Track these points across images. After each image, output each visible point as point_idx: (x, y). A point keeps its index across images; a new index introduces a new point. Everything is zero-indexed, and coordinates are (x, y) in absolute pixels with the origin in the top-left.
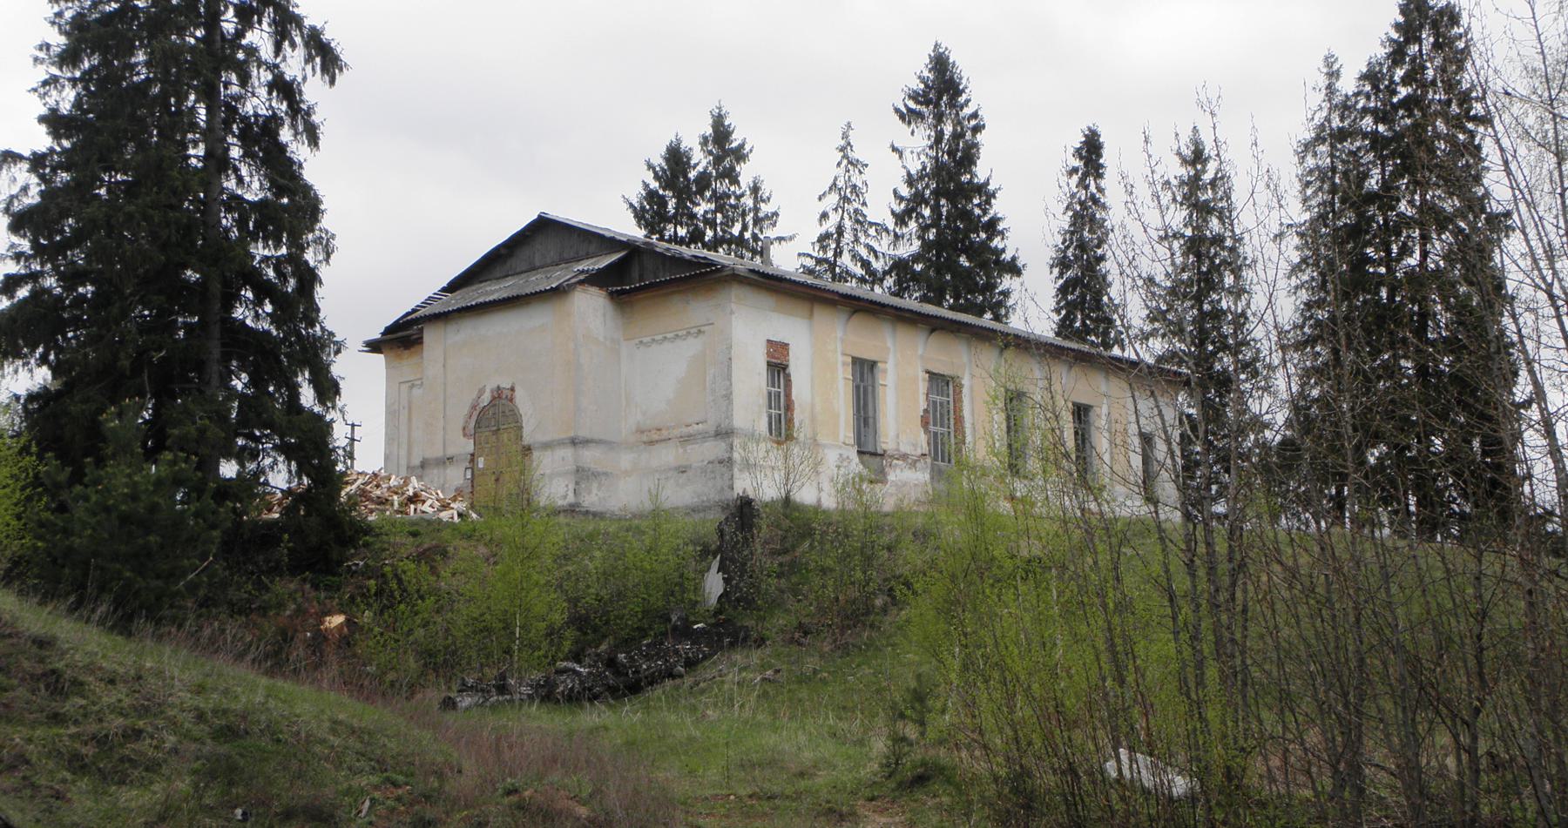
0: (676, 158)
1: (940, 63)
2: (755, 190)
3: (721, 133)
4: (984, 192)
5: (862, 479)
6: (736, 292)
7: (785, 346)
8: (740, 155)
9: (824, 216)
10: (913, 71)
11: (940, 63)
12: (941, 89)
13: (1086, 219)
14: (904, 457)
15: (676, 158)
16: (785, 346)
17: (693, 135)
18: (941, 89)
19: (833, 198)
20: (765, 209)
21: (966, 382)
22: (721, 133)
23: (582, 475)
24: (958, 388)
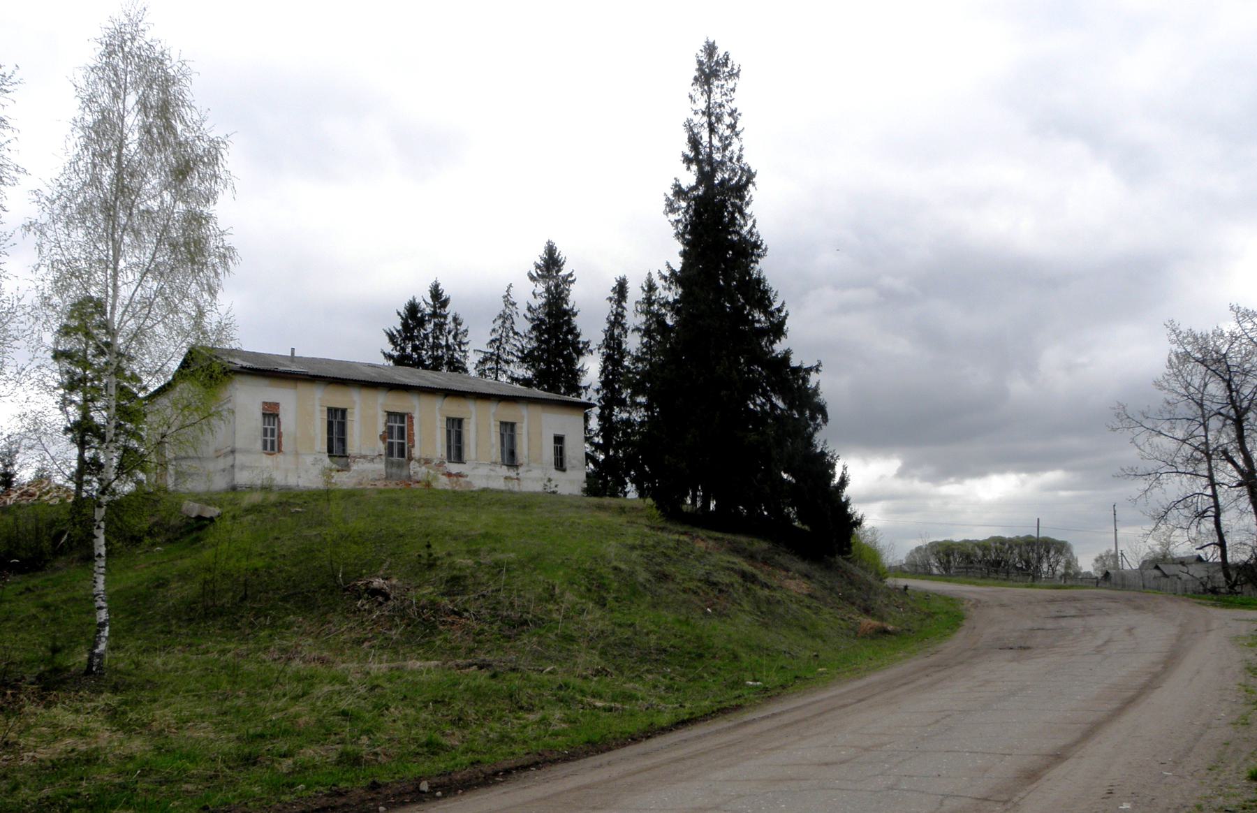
0: (413, 309)
1: (551, 250)
2: (455, 319)
3: (436, 293)
4: (571, 313)
5: (331, 470)
6: (238, 378)
7: (277, 405)
8: (444, 304)
9: (494, 330)
10: (537, 254)
11: (551, 250)
12: (551, 262)
13: (617, 321)
14: (365, 457)
15: (413, 309)
16: (277, 405)
17: (424, 299)
18: (551, 262)
19: (500, 322)
20: (462, 328)
21: (416, 416)
22: (436, 293)
23: (179, 475)
24: (411, 418)
